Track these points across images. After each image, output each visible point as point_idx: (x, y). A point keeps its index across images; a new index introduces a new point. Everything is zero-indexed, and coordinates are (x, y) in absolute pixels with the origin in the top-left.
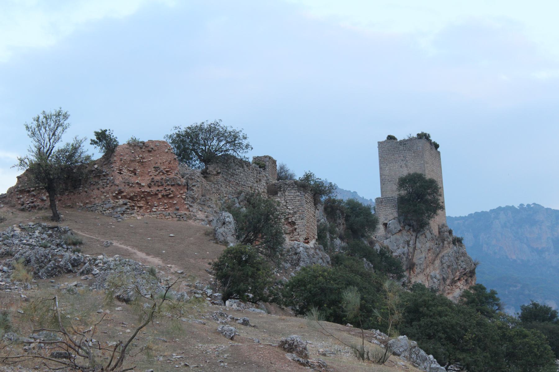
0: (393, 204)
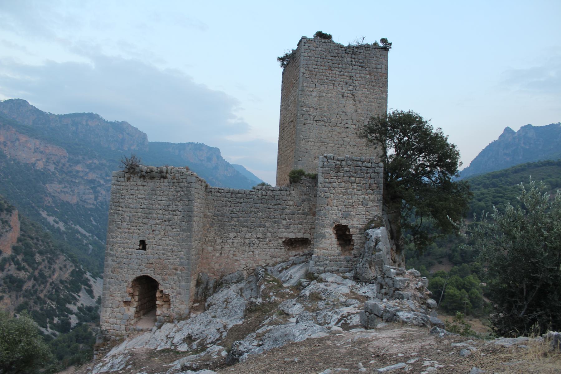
0: (372, 181)
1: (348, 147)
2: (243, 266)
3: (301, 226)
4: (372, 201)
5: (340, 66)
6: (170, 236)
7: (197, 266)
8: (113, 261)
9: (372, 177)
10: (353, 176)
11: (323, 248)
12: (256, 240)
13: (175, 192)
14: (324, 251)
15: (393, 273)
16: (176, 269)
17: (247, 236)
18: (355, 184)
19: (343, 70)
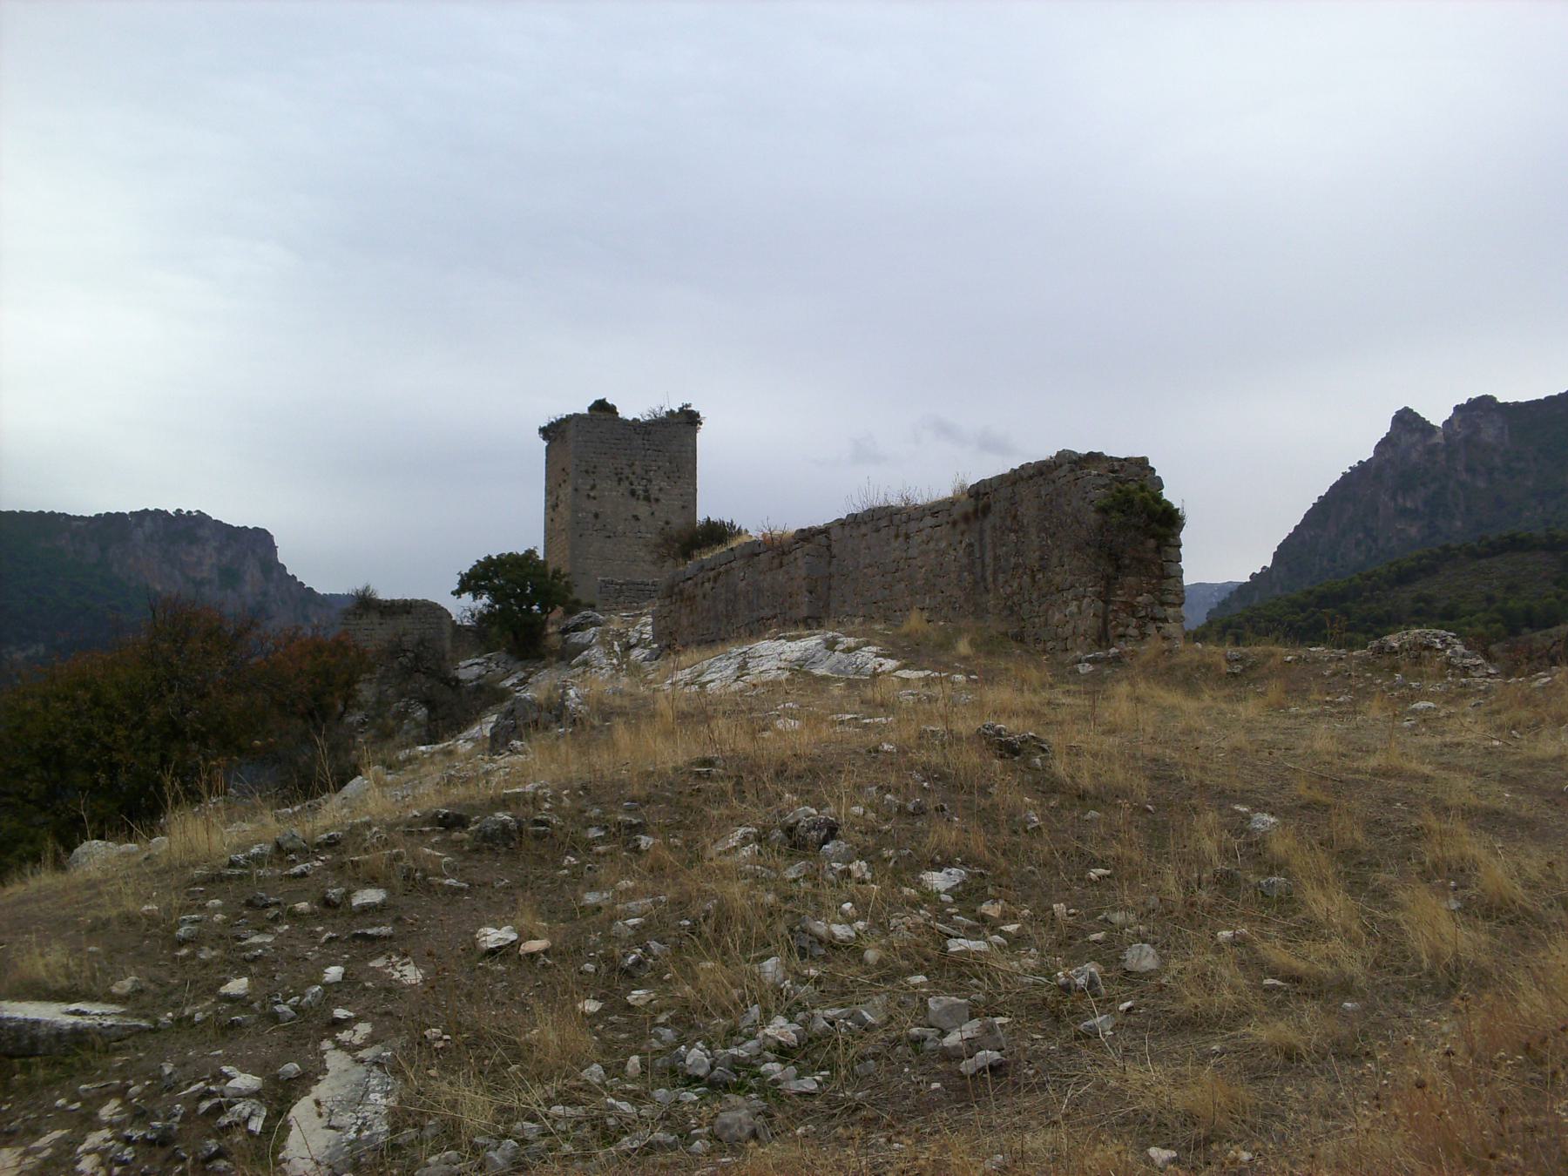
1: (642, 564)
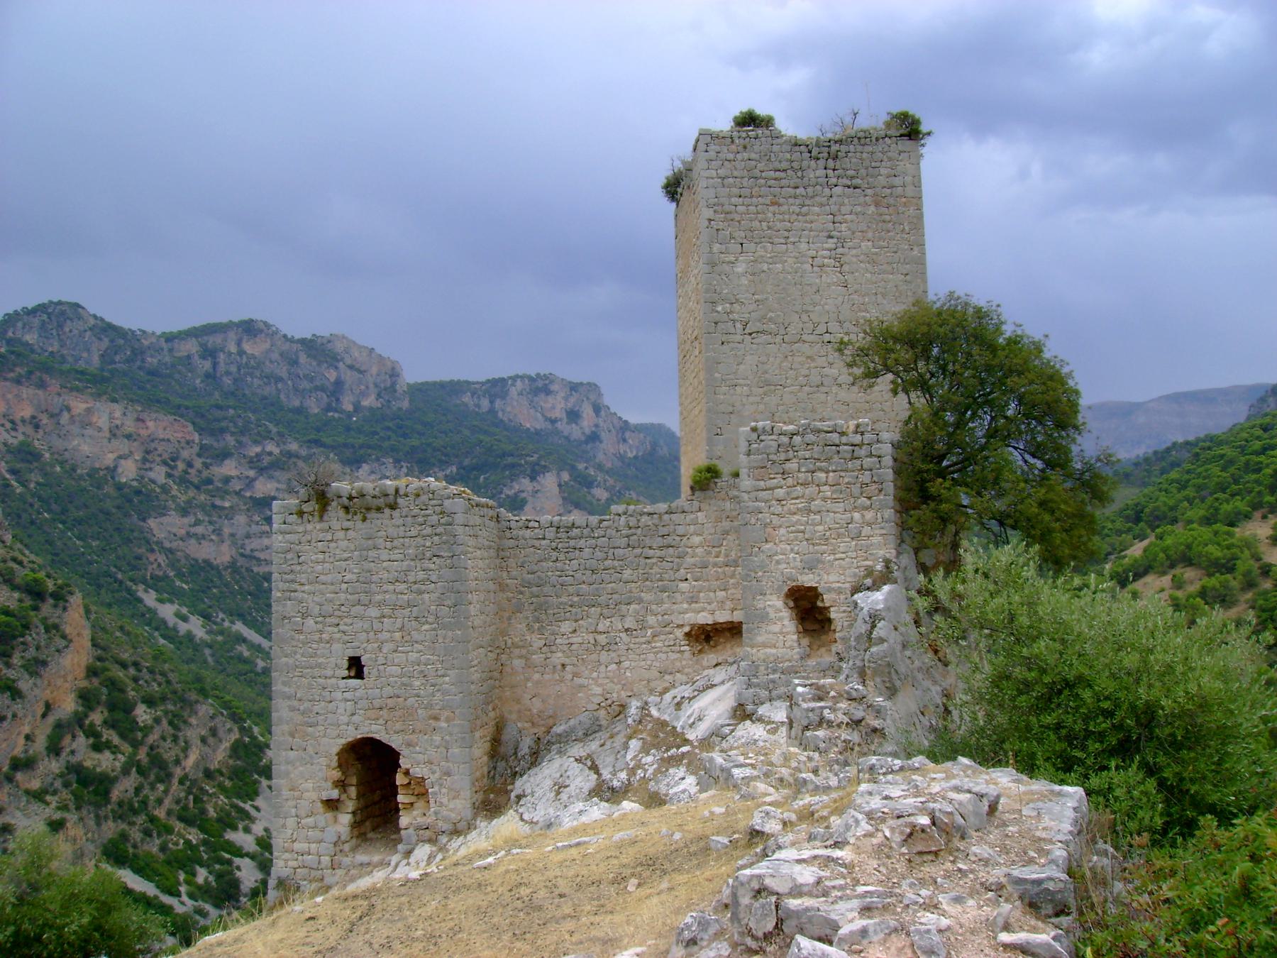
0: (866, 477)
1: (835, 389)
2: (597, 700)
3: (723, 593)
4: (869, 524)
5: (798, 191)
6: (416, 642)
7: (490, 708)
8: (292, 709)
9: (865, 466)
10: (821, 469)
11: (763, 642)
12: (623, 635)
13: (419, 539)
14: (768, 650)
15: (800, 694)
16: (436, 718)
17: (601, 628)
18: (826, 488)
19: (807, 202)
